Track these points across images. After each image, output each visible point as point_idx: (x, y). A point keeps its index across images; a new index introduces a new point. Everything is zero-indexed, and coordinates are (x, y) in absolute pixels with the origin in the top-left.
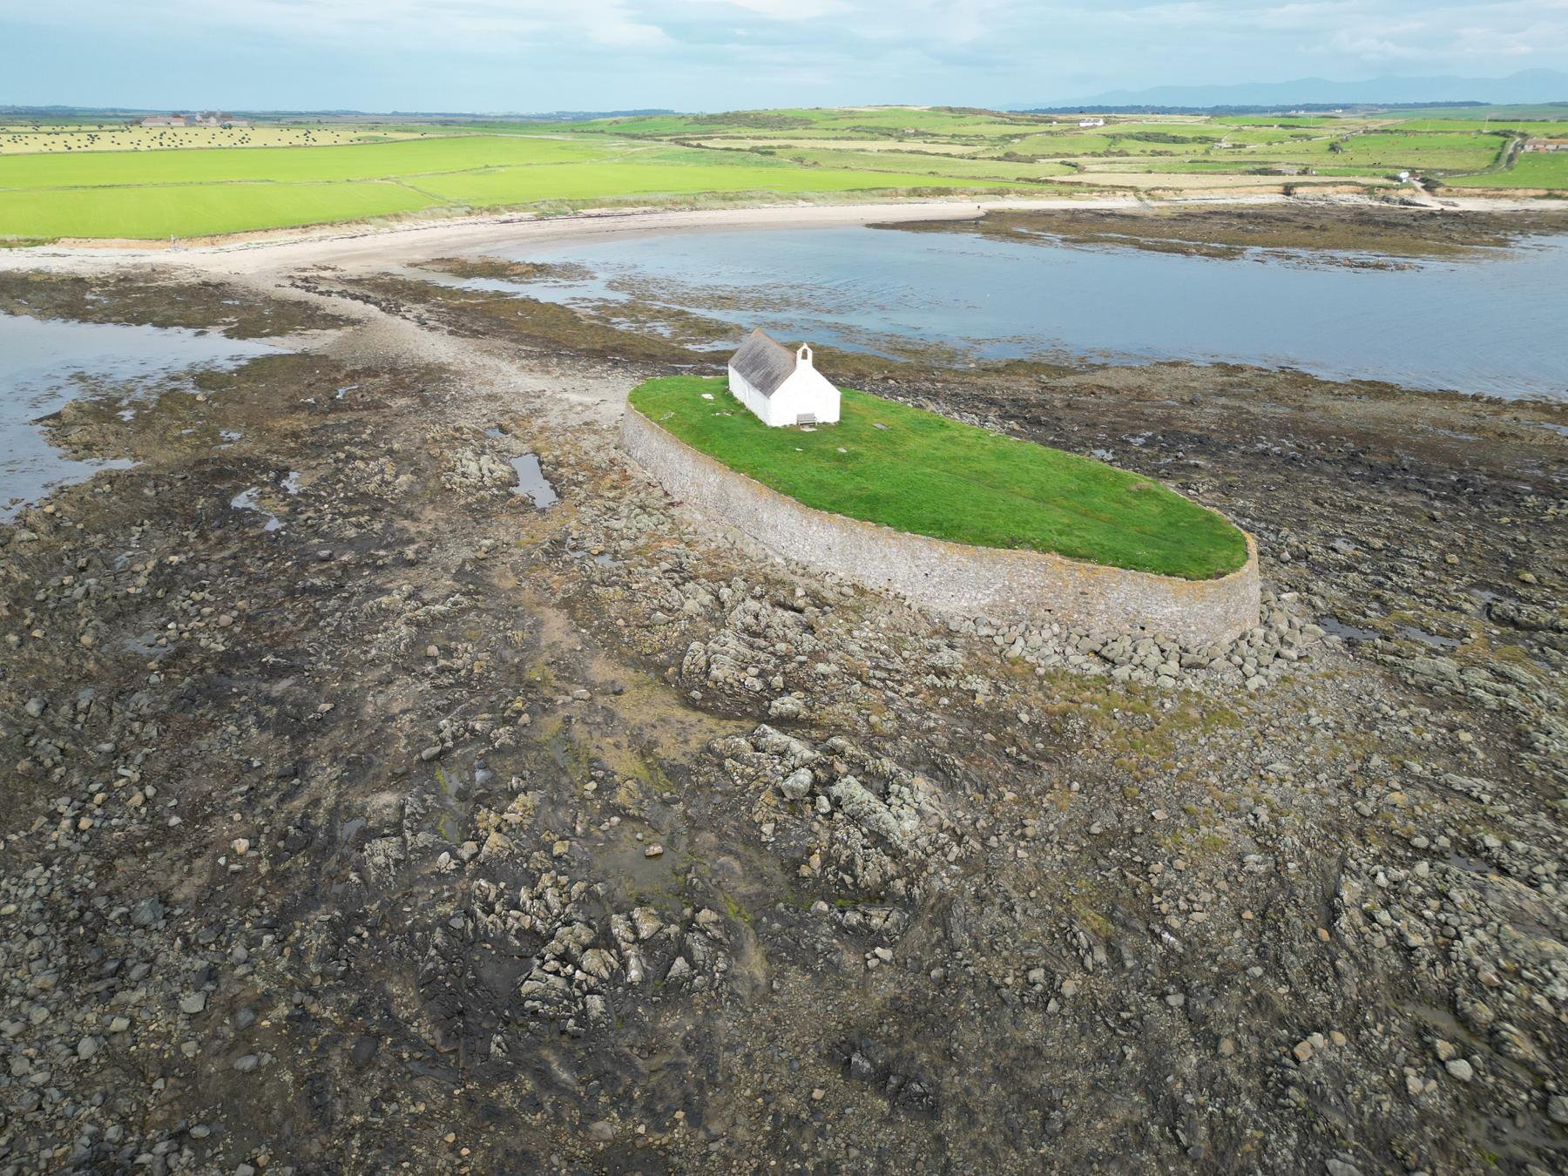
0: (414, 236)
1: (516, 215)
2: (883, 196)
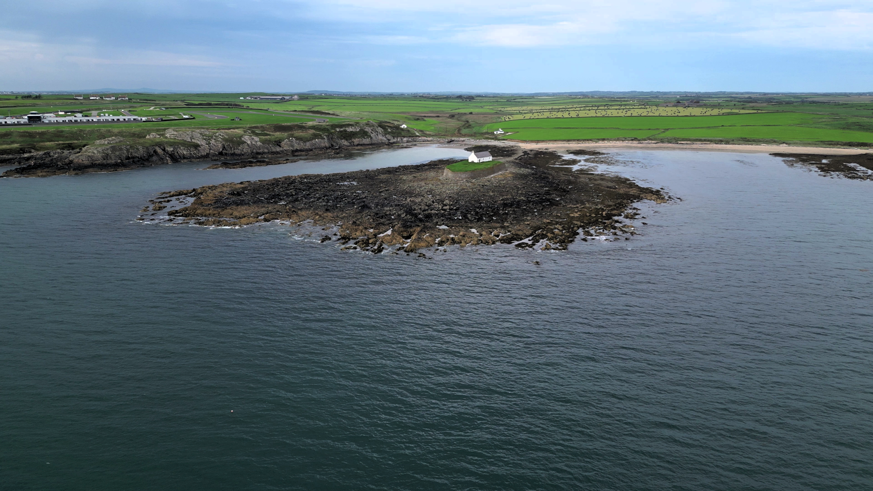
1: (650, 141)
2: (830, 144)
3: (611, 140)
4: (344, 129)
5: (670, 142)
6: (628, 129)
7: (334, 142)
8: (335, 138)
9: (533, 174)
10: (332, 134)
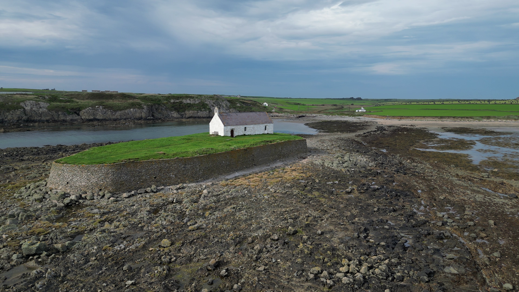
0: (487, 123)
3: (498, 118)
4: (180, 100)
7: (159, 113)
8: (162, 109)
10: (159, 105)
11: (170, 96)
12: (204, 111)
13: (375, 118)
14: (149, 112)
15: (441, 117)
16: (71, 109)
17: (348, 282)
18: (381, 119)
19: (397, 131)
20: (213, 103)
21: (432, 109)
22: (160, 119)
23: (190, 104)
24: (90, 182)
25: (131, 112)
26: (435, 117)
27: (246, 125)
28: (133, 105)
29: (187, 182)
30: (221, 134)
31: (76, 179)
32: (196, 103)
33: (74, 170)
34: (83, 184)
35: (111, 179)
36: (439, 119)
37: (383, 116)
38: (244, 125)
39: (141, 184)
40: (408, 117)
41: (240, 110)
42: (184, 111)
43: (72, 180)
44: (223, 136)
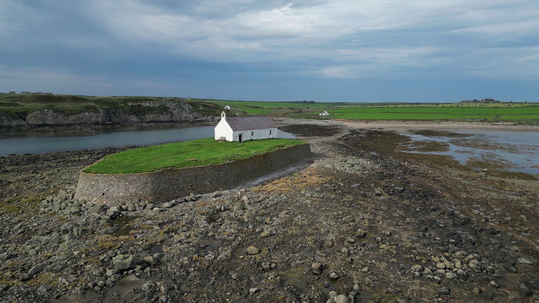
0: (446, 125)
1: (505, 123)
3: (455, 121)
4: (139, 103)
5: (531, 125)
6: (458, 114)
7: (117, 117)
8: (119, 113)
9: (382, 176)
10: (116, 108)
11: (126, 99)
12: (165, 115)
13: (342, 121)
14: (106, 117)
15: (404, 120)
16: (16, 114)
17: (453, 277)
18: (349, 123)
19: (371, 134)
20: (175, 106)
21: (390, 112)
22: (118, 124)
23: (150, 107)
24: (128, 192)
25: (86, 116)
26: (399, 120)
27: (253, 129)
28: (87, 109)
29: (221, 189)
30: (230, 138)
31: (113, 190)
32: (156, 106)
33: (110, 180)
34: (120, 194)
35: (150, 188)
36: (403, 122)
37: (351, 120)
38: (251, 130)
39: (179, 193)
40: (374, 120)
41: (204, 113)
42: (144, 115)
43: (108, 190)
44: (232, 142)
